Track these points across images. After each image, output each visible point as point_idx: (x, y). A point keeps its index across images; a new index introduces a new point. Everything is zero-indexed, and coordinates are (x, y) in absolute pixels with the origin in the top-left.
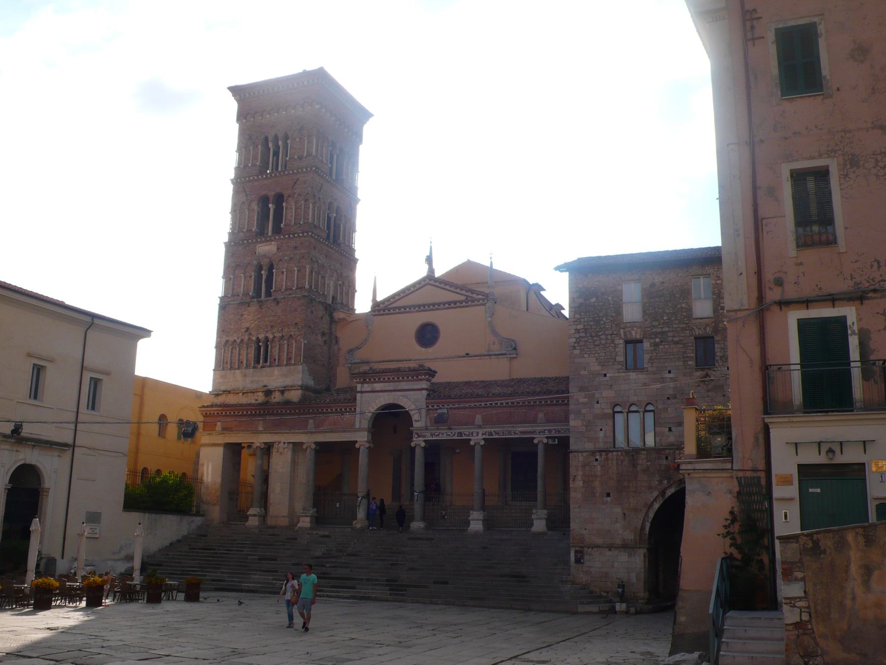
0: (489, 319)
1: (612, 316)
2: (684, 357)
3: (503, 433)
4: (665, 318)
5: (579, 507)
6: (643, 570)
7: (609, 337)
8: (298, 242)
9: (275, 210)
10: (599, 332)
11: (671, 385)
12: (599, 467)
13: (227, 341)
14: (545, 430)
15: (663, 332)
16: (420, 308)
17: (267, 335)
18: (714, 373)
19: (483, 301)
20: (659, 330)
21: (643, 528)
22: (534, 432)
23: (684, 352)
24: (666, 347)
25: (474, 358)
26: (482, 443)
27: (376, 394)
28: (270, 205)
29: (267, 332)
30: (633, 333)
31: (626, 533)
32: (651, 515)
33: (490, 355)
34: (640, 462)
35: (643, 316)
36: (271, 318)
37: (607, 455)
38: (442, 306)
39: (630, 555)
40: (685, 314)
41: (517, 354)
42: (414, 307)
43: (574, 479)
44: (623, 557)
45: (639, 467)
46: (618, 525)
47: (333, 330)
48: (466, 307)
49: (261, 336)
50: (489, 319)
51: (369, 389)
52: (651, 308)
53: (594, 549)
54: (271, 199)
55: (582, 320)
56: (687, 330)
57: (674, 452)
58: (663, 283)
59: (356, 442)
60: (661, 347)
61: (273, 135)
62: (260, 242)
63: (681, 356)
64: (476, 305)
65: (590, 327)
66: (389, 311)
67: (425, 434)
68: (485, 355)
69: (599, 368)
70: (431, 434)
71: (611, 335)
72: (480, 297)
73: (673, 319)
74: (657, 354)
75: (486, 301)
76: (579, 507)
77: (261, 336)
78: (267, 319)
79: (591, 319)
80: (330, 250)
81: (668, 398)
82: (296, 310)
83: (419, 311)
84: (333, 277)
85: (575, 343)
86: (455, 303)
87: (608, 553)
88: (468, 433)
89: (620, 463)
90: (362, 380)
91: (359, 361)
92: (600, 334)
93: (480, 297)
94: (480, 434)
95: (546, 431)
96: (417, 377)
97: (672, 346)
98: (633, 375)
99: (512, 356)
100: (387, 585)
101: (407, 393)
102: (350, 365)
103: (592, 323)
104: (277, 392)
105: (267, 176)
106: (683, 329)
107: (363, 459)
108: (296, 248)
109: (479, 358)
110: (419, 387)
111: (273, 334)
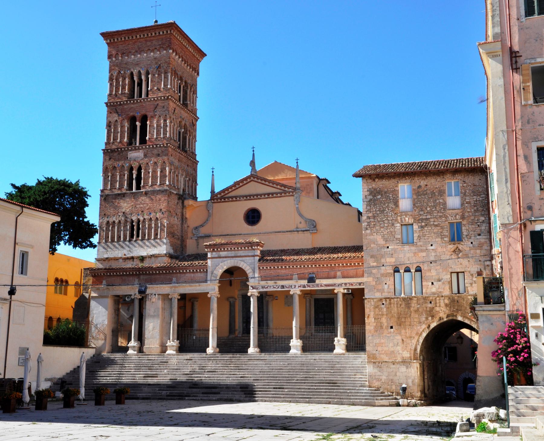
0: (297, 206)
1: (392, 208)
2: (441, 235)
3: (313, 286)
4: (428, 209)
5: (372, 336)
6: (416, 377)
7: (390, 222)
8: (160, 151)
9: (141, 127)
10: (383, 218)
11: (433, 254)
12: (385, 309)
13: (108, 222)
14: (342, 284)
15: (427, 218)
16: (247, 198)
17: (139, 217)
18: (462, 246)
19: (293, 193)
20: (424, 217)
21: (415, 350)
22: (335, 285)
23: (441, 232)
24: (429, 228)
25: (286, 233)
26: (299, 293)
27: (221, 259)
29: (138, 215)
30: (407, 219)
31: (404, 353)
32: (421, 340)
33: (298, 231)
34: (413, 305)
35: (413, 208)
37: (390, 300)
38: (263, 196)
39: (407, 367)
40: (441, 206)
41: (317, 230)
42: (243, 197)
43: (368, 317)
44: (403, 369)
45: (412, 309)
46: (399, 348)
47: (184, 213)
48: (280, 197)
50: (297, 206)
51: (216, 256)
52: (419, 203)
53: (383, 364)
54: (138, 119)
55: (372, 210)
56: (444, 217)
57: (436, 298)
58: (426, 185)
59: (208, 293)
60: (426, 228)
62: (131, 150)
63: (439, 235)
64: (287, 196)
65: (377, 215)
66: (225, 199)
68: (294, 231)
69: (384, 243)
71: (391, 220)
72: (290, 190)
73: (434, 209)
74: (423, 233)
75: (294, 193)
76: (372, 336)
77: (134, 218)
78: (138, 206)
79: (378, 209)
80: (181, 155)
81: (431, 263)
82: (160, 200)
83: (247, 200)
84: (183, 175)
85: (367, 225)
86: (272, 194)
87: (392, 366)
88: (288, 286)
89: (399, 306)
90: (212, 250)
91: (203, 235)
92: (384, 219)
93: (290, 190)
94: (297, 287)
95: (343, 284)
96: (252, 247)
97: (433, 228)
98: (407, 248)
99: (313, 232)
100: (243, 391)
101: (244, 258)
102: (196, 238)
103: (378, 212)
104: (147, 258)
105: (134, 102)
106: (440, 217)
107: (214, 305)
109: (290, 233)
110: (252, 254)
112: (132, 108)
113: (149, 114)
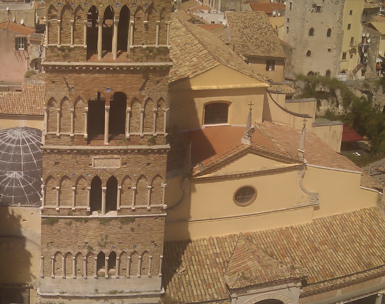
28: (107, 107)
36: (119, 236)
49: (106, 251)
61: (106, 6)
82: (151, 229)
108: (148, 164)
111: (121, 249)
112: (96, 78)
113: (130, 95)
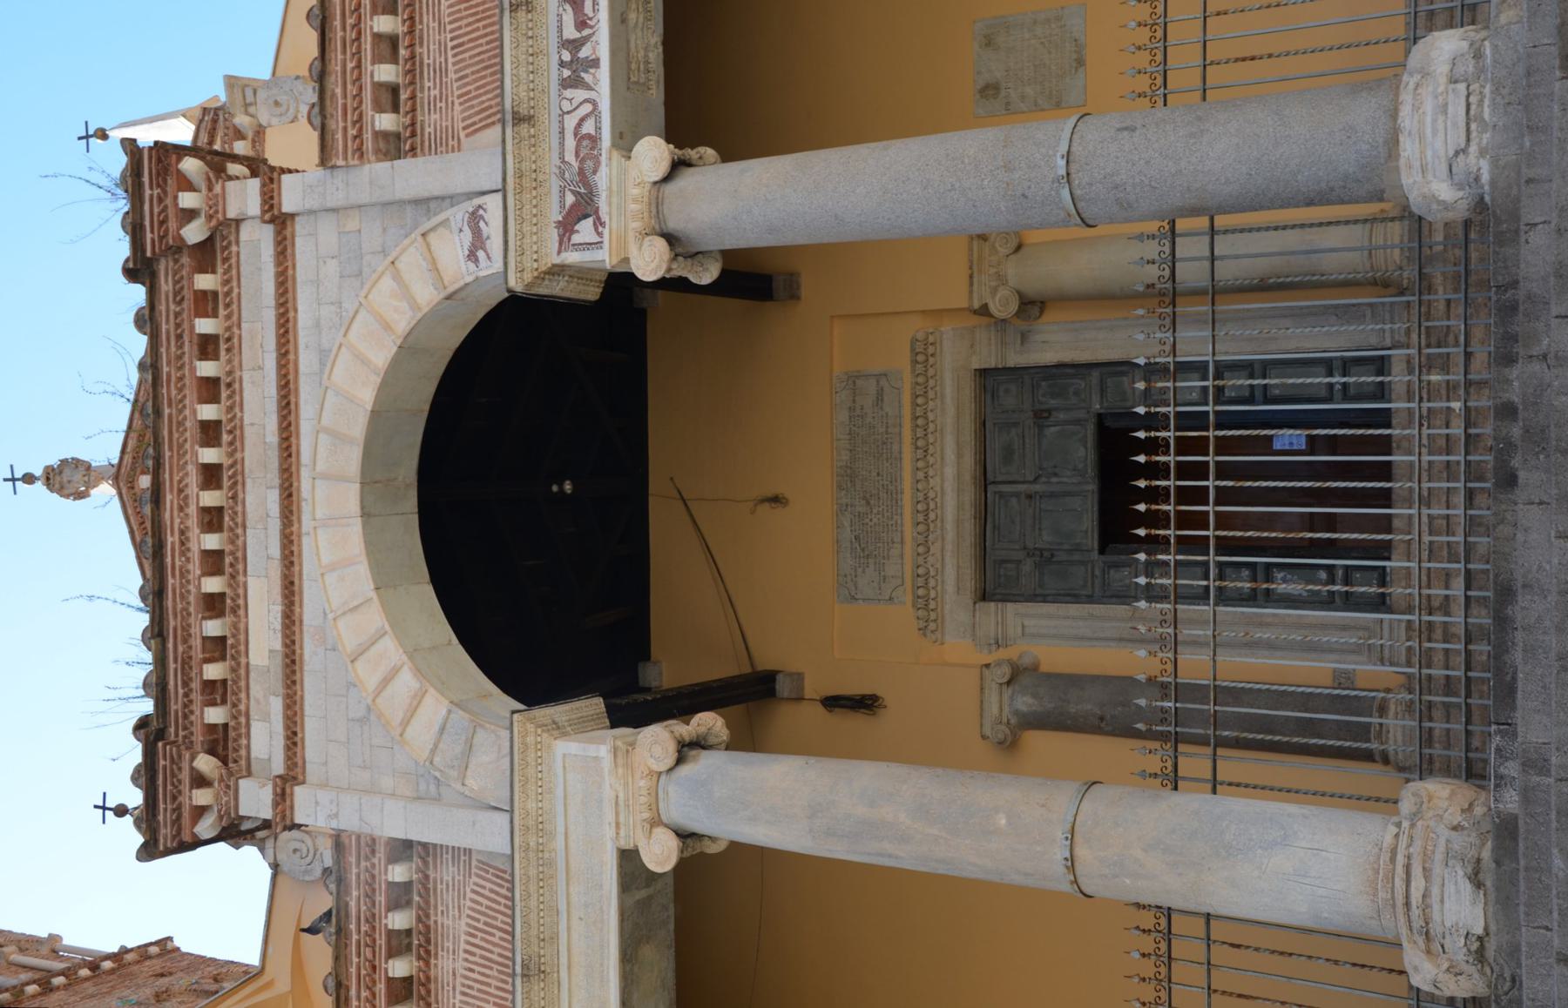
59: (629, 859)
67: (570, 143)
70: (575, 82)
75: (241, 120)
90: (205, 763)
101: (306, 361)
